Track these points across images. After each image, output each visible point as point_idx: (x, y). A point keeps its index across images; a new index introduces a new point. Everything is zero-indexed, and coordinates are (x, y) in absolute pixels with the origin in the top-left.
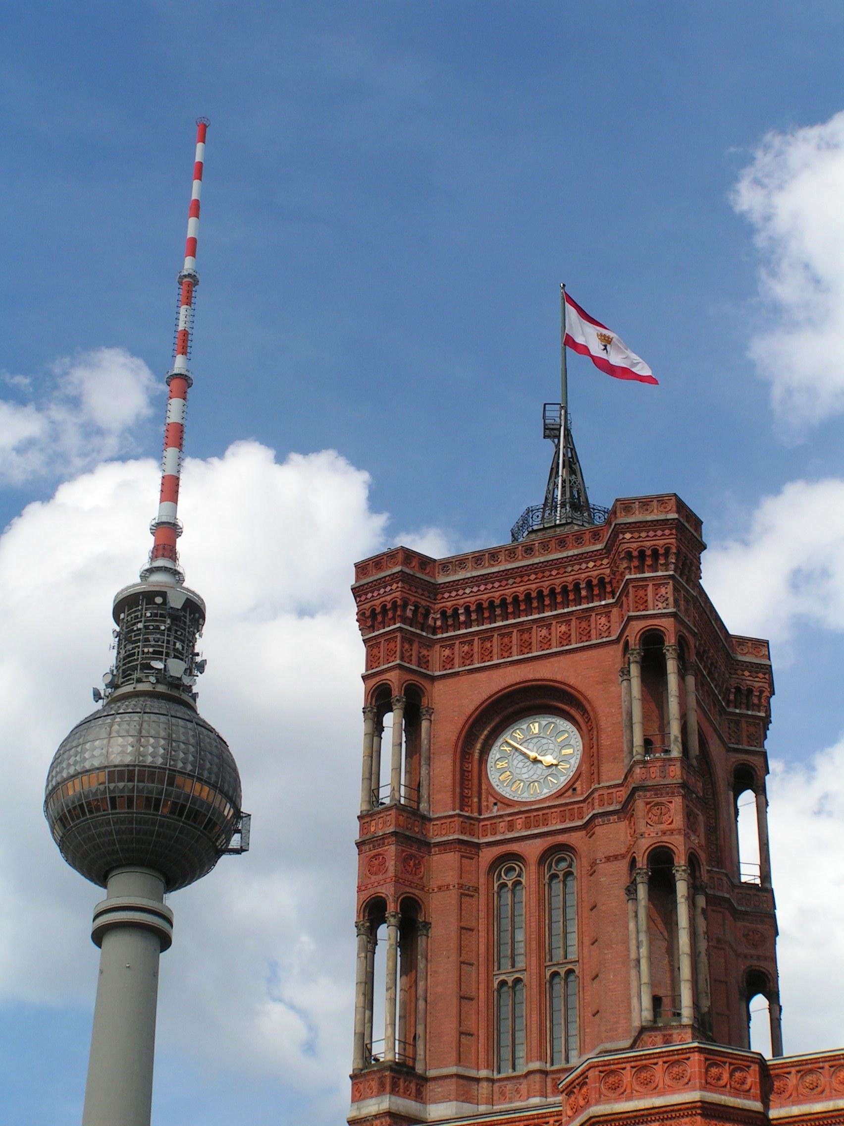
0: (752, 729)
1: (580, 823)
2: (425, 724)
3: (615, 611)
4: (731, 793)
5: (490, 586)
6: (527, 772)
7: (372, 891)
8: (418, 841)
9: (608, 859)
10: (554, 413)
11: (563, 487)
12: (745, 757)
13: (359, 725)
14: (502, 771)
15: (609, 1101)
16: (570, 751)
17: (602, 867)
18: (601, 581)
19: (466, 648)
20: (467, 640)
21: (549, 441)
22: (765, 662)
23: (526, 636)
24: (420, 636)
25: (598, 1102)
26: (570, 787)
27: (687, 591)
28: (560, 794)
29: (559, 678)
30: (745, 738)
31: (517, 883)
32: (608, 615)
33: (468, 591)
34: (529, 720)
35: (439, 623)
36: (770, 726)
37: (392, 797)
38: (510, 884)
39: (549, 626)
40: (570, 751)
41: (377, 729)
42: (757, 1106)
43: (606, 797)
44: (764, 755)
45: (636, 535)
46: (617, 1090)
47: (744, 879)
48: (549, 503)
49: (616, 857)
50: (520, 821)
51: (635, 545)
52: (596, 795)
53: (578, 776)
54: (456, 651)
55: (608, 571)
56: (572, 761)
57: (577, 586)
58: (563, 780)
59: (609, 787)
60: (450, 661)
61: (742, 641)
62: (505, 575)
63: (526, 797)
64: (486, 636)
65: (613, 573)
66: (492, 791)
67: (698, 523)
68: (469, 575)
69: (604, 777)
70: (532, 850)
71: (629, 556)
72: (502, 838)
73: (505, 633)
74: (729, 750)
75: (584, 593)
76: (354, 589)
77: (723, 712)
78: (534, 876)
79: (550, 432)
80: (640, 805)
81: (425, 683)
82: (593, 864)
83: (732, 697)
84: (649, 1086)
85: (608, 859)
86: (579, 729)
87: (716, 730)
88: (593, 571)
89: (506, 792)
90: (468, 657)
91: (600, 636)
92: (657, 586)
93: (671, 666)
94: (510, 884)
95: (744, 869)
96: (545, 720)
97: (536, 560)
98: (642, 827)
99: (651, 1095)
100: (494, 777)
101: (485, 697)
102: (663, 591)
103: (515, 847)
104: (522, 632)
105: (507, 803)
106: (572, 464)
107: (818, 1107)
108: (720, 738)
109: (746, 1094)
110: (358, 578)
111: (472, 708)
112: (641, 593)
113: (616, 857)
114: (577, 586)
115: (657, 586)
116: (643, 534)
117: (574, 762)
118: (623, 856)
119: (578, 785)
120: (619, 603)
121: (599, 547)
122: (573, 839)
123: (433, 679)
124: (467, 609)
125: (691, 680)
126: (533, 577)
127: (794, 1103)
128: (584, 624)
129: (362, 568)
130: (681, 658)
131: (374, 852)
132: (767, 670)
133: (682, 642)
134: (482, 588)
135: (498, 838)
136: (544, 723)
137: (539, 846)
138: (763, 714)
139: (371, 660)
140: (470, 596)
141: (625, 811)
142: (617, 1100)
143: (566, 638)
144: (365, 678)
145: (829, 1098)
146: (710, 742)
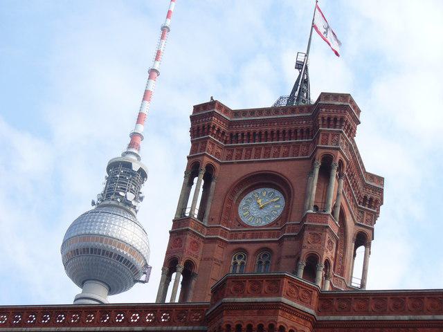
0: (369, 217)
1: (277, 239)
2: (213, 184)
3: (312, 145)
4: (354, 244)
5: (255, 126)
6: (256, 213)
7: (173, 255)
8: (197, 235)
9: (287, 257)
10: (301, 58)
11: (300, 91)
12: (363, 229)
13: (180, 179)
14: (245, 211)
15: (233, 296)
16: (279, 206)
17: (283, 261)
18: (308, 129)
19: (239, 152)
20: (240, 149)
21: (297, 70)
22: (381, 187)
23: (268, 151)
24: (218, 143)
25: (227, 296)
26: (276, 222)
27: (347, 140)
28: (270, 225)
29: (279, 171)
30: (365, 220)
31: (242, 263)
32: (308, 146)
33: (244, 126)
34: (262, 189)
35: (228, 139)
36: (378, 218)
37: (190, 213)
38: (239, 263)
39: (279, 148)
40: (279, 206)
41: (188, 184)
42: (312, 312)
43: (291, 229)
44: (373, 230)
45: (328, 110)
46: (240, 291)
47: (353, 284)
48: (291, 97)
49: (291, 257)
50: (248, 235)
51: (327, 115)
52: (287, 227)
53: (280, 218)
54: (234, 153)
55: (311, 126)
56: (279, 211)
57: (296, 131)
58: (273, 219)
59: (293, 224)
60: (229, 157)
61: (372, 177)
62: (263, 122)
63: (253, 224)
64: (249, 148)
65: (314, 127)
66: (238, 219)
67: (359, 111)
68: (247, 119)
69: (292, 219)
70: (252, 249)
71: (323, 118)
72: (239, 240)
73: (258, 148)
74: (356, 224)
75: (298, 134)
76: (191, 117)
77: (356, 206)
78: (250, 261)
79: (299, 66)
80: (307, 233)
81: (217, 166)
82: (279, 259)
83: (362, 201)
84: (256, 291)
85: (287, 257)
86: (285, 198)
87: (351, 213)
88: (304, 124)
89: (245, 220)
90: (239, 157)
91: (303, 155)
92: (333, 135)
93: (335, 173)
94: (239, 263)
95: (353, 280)
96: (269, 190)
97: (279, 116)
98: (305, 244)
99: (256, 296)
100: (241, 213)
101: (243, 175)
102: (336, 138)
103: (244, 246)
104: (266, 148)
105: (245, 226)
106: (306, 82)
107: (344, 318)
108: (353, 217)
109: (309, 305)
110: (194, 112)
111: (236, 179)
112: (325, 137)
113: (291, 257)
114: (296, 131)
115: (333, 135)
116: (331, 110)
117: (280, 212)
118: (294, 257)
119: (279, 222)
120: (315, 142)
121: (309, 114)
122: (273, 246)
123: (221, 164)
124: (243, 135)
125: (342, 182)
126: (276, 124)
127: (332, 315)
128: (296, 149)
129: (197, 108)
130: (339, 169)
131: (177, 237)
132: (381, 191)
133: (341, 162)
134: (251, 126)
135: (237, 240)
136: (269, 192)
137: (257, 246)
138: (375, 211)
139: (192, 151)
140: (245, 129)
141: (299, 237)
142: (238, 296)
143: (286, 154)
144: (188, 158)
145: (351, 314)
146: (347, 217)
